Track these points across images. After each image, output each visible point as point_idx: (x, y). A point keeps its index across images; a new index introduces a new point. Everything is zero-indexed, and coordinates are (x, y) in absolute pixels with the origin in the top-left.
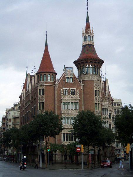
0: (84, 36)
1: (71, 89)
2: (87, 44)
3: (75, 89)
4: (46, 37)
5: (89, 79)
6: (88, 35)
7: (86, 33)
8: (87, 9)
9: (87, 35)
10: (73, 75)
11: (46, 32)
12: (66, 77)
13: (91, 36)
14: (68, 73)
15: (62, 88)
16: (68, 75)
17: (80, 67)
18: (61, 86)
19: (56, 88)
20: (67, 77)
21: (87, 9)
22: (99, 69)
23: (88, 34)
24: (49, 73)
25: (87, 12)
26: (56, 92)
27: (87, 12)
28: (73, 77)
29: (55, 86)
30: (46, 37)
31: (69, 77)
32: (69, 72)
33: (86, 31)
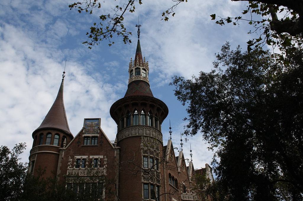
1: (91, 157)
3: (102, 157)
4: (63, 80)
6: (135, 68)
8: (139, 36)
10: (99, 131)
11: (64, 73)
12: (83, 136)
14: (90, 128)
15: (73, 157)
18: (71, 152)
19: (60, 157)
20: (86, 135)
21: (139, 36)
24: (50, 131)
26: (60, 165)
28: (98, 135)
29: (58, 155)
30: (63, 80)
31: (90, 135)
32: (90, 126)
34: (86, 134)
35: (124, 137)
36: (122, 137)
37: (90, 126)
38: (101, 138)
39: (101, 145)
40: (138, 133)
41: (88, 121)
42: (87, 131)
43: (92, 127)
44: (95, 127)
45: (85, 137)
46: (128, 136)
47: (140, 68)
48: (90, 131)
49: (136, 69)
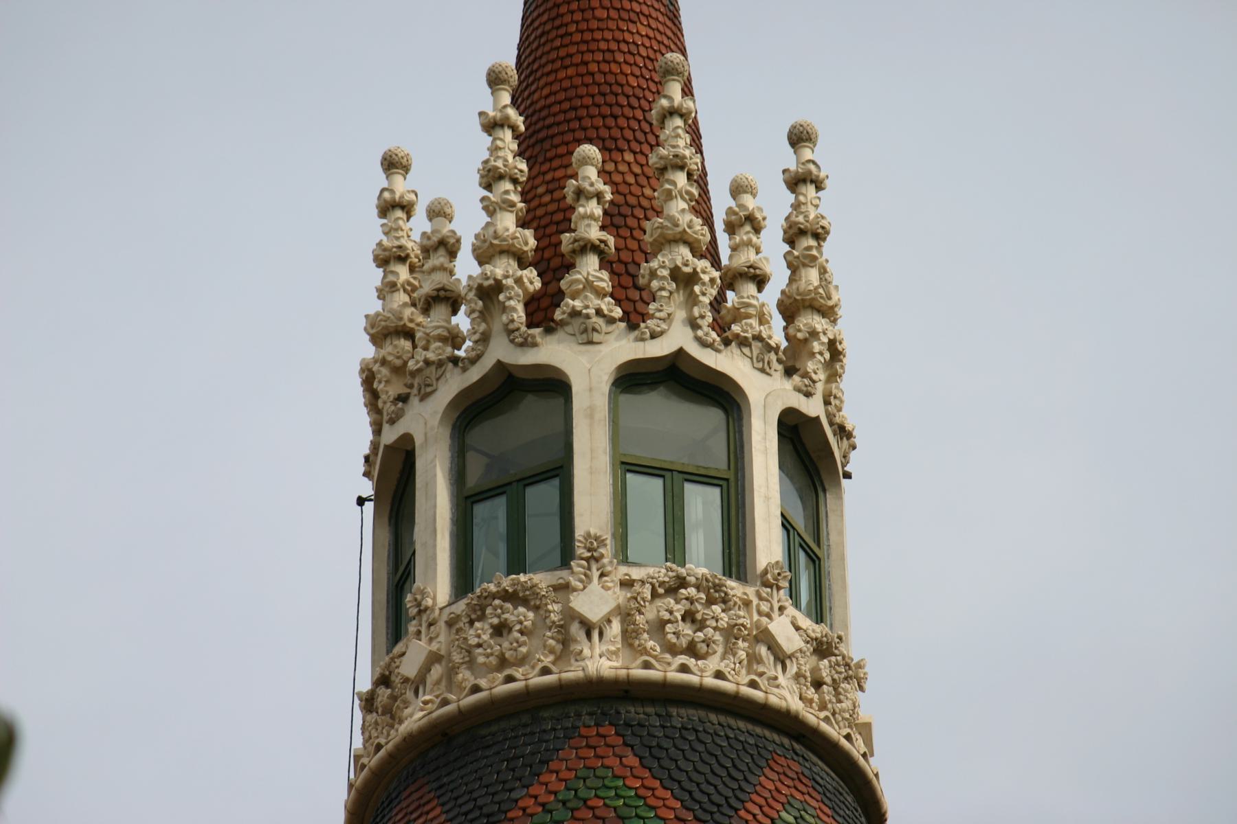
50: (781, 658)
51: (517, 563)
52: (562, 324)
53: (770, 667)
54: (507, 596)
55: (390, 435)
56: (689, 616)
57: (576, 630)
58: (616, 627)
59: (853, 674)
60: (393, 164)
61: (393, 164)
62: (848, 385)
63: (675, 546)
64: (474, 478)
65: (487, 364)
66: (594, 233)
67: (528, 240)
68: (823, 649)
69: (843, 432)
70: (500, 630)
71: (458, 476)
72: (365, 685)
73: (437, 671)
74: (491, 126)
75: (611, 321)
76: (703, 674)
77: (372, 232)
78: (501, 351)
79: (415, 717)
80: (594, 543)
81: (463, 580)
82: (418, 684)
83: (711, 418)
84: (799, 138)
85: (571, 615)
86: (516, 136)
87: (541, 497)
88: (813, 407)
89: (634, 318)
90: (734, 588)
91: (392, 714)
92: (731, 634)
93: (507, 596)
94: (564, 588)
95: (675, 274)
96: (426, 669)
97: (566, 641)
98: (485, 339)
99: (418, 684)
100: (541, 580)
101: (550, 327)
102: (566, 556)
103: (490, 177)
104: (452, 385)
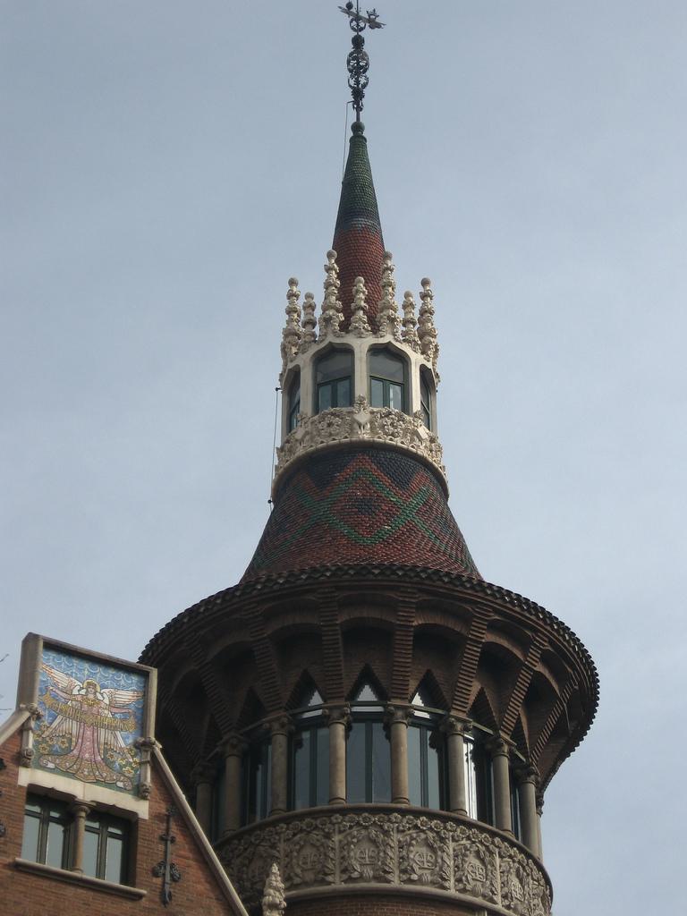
0: (305, 362)
2: (365, 435)
5: (396, 882)
6: (371, 340)
7: (348, 312)
8: (358, 94)
9: (361, 345)
12: (26, 777)
13: (416, 359)
14: (74, 727)
16: (63, 756)
17: (255, 708)
21: (358, 94)
22: (532, 789)
23: (375, 329)
25: (357, 128)
27: (357, 128)
28: (142, 809)
32: (77, 715)
33: (346, 296)
34: (44, 768)
35: (338, 884)
36: (310, 876)
37: (77, 715)
38: (164, 839)
39: (165, 899)
40: (459, 880)
41: (64, 660)
42: (58, 744)
43: (97, 725)
44: (112, 728)
45: (38, 795)
46: (377, 878)
47: (402, 359)
48: (79, 758)
49: (375, 350)
50: (421, 439)
51: (334, 405)
52: (352, 331)
53: (417, 442)
54: (332, 414)
55: (291, 366)
56: (392, 424)
57: (356, 426)
58: (369, 426)
59: (440, 450)
60: (292, 282)
61: (292, 282)
62: (438, 361)
63: (386, 403)
64: (319, 380)
65: (326, 343)
66: (363, 304)
67: (339, 304)
68: (432, 440)
69: (437, 375)
70: (330, 425)
71: (315, 378)
72: (279, 445)
73: (307, 437)
74: (328, 269)
75: (368, 331)
76: (397, 442)
77: (286, 303)
78: (331, 339)
79: (300, 451)
80: (362, 399)
81: (316, 410)
82: (301, 441)
83: (398, 365)
84: (425, 283)
85: (354, 421)
86: (336, 273)
87: (342, 387)
88: (429, 365)
89: (375, 329)
90: (407, 417)
91: (291, 451)
92: (406, 431)
93: (332, 414)
94: (351, 413)
95: (389, 317)
96: (304, 436)
97: (352, 429)
98: (325, 335)
99: (301, 441)
100: (345, 410)
101: (348, 332)
102: (351, 403)
103: (328, 285)
104: (314, 349)
